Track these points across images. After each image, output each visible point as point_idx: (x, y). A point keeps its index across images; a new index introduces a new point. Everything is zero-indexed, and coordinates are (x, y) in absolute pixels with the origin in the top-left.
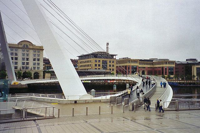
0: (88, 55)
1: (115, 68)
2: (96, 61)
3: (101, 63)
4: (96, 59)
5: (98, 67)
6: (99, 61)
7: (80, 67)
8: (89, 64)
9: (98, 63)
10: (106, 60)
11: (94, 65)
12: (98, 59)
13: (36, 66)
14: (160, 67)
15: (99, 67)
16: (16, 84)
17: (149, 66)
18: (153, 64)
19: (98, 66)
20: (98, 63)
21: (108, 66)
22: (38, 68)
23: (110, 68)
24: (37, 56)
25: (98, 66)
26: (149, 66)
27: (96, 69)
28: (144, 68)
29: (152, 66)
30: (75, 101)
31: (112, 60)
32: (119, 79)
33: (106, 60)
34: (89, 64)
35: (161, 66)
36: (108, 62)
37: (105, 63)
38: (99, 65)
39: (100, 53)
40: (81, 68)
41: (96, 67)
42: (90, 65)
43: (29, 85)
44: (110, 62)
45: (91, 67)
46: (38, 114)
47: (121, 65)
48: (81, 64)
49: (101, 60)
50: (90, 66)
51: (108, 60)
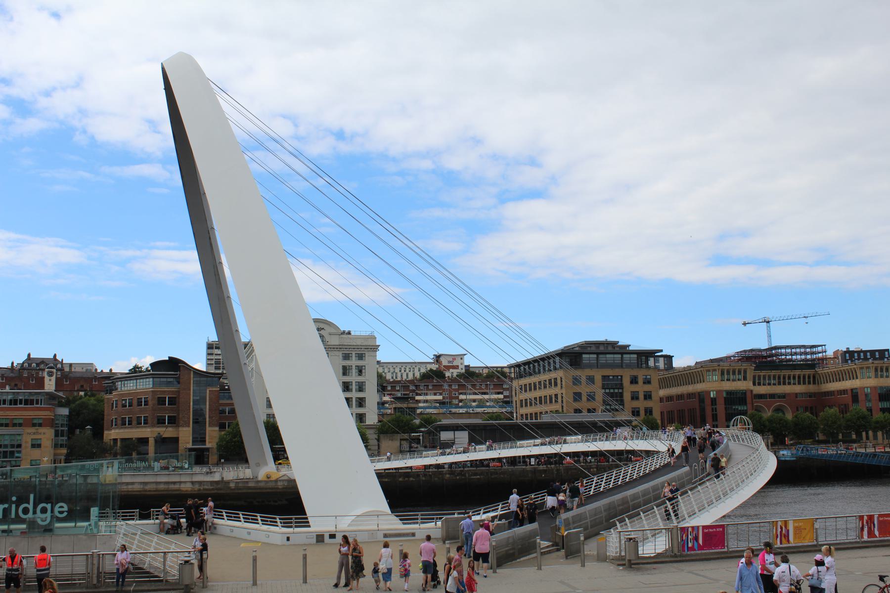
0: (548, 358)
2: (576, 381)
4: (578, 373)
5: (584, 404)
7: (522, 406)
9: (584, 389)
10: (617, 372)
11: (569, 398)
12: (583, 374)
14: (844, 392)
15: (590, 405)
16: (274, 478)
17: (798, 389)
18: (814, 379)
19: (584, 398)
21: (627, 396)
23: (635, 404)
24: (354, 371)
25: (584, 398)
26: (798, 389)
27: (589, 411)
28: (783, 396)
29: (812, 388)
30: (317, 536)
31: (641, 374)
32: (628, 448)
33: (617, 372)
35: (848, 384)
36: (626, 381)
38: (591, 397)
39: (593, 349)
40: (524, 411)
41: (577, 405)
42: (556, 395)
44: (634, 381)
46: (156, 574)
48: (524, 396)
49: (598, 375)
50: (556, 401)
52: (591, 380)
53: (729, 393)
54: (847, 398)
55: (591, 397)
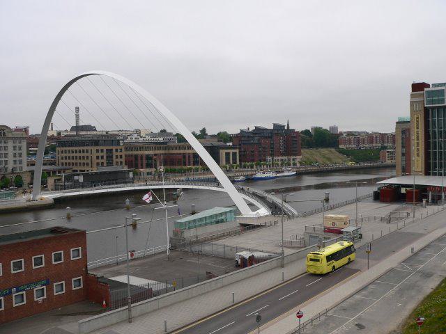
1: (123, 160)
2: (97, 151)
3: (104, 154)
4: (98, 148)
6: (102, 151)
8: (85, 155)
11: (95, 157)
12: (100, 148)
13: (18, 165)
14: (180, 154)
17: (162, 152)
20: (100, 154)
21: (114, 157)
22: (21, 168)
26: (162, 152)
29: (166, 152)
34: (85, 155)
35: (182, 151)
36: (114, 151)
37: (109, 151)
43: (55, 200)
45: (89, 161)
47: (131, 153)
48: (64, 155)
49: (105, 148)
51: (114, 148)
52: (102, 151)
53: (147, 155)
54: (181, 157)
55: (102, 157)
